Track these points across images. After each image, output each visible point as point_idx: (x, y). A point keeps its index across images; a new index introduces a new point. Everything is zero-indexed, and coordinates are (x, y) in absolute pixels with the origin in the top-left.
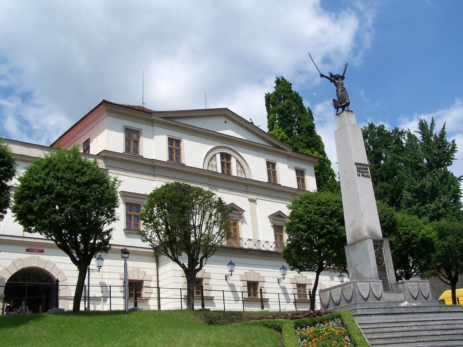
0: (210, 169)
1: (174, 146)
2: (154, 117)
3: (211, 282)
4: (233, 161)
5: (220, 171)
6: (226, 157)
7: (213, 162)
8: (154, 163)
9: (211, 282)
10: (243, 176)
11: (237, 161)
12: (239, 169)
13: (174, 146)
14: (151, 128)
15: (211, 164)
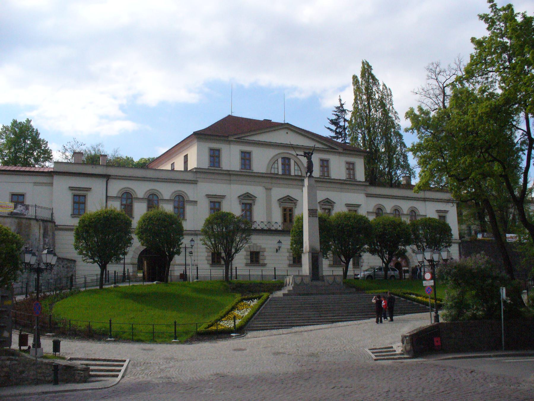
0: (273, 172)
1: (246, 158)
2: (229, 139)
3: (265, 254)
4: (292, 162)
5: (280, 172)
6: (286, 161)
7: (276, 165)
8: (230, 173)
9: (265, 254)
10: (300, 174)
11: (295, 162)
12: (296, 167)
13: (246, 158)
14: (228, 146)
15: (273, 167)
